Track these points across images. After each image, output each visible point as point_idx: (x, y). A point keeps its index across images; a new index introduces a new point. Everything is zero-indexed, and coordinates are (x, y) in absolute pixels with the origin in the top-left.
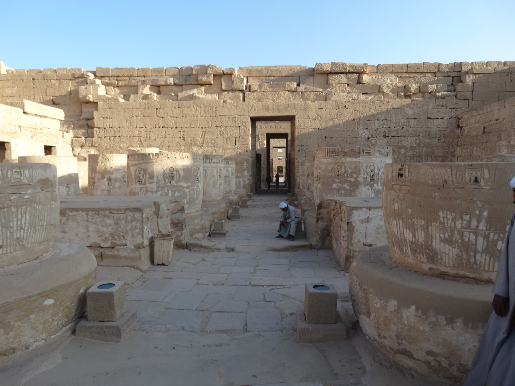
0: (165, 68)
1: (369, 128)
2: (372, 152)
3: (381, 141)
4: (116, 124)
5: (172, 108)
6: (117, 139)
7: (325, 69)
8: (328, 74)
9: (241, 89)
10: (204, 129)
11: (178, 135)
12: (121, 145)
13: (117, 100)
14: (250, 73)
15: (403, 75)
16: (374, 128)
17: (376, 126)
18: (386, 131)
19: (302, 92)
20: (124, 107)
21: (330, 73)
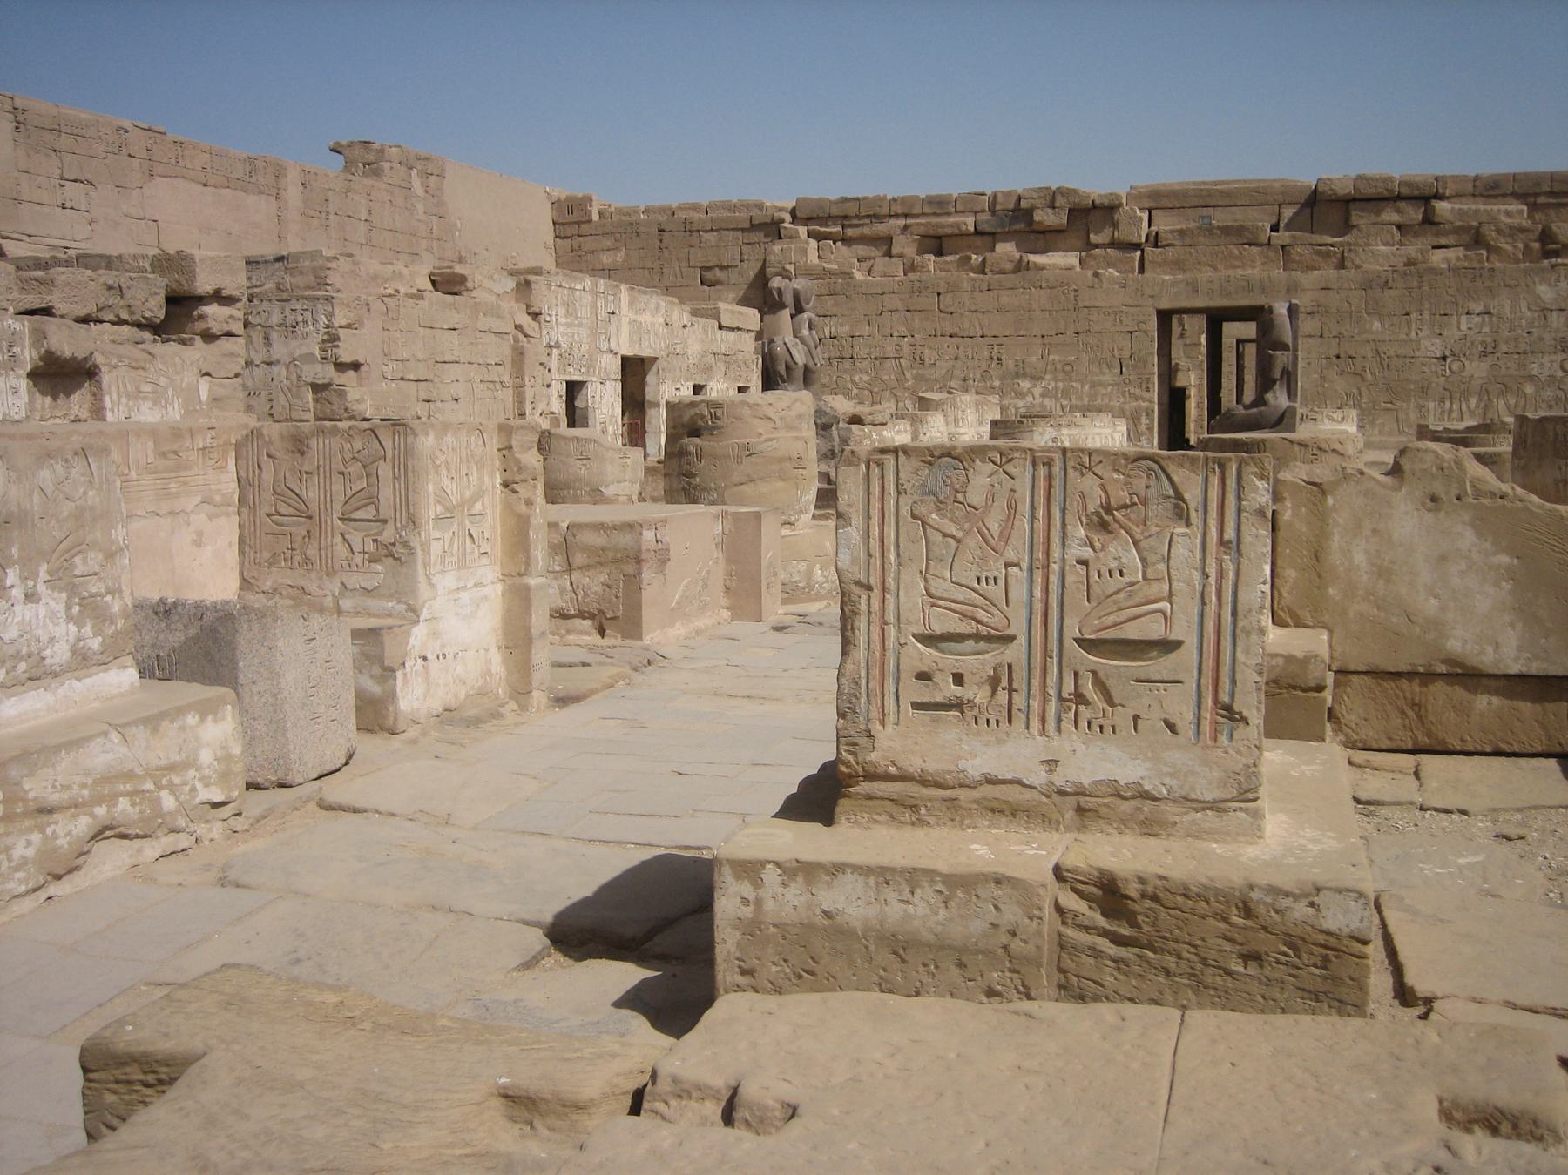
0: (955, 195)
1: (1445, 333)
2: (1319, 417)
3: (1475, 364)
4: (844, 330)
5: (973, 290)
6: (847, 364)
7: (1341, 192)
8: (1348, 201)
9: (1135, 240)
10: (1046, 340)
11: (986, 354)
12: (857, 378)
13: (850, 275)
14: (1158, 200)
15: (1541, 200)
16: (1457, 335)
17: (1464, 327)
18: (1489, 340)
19: (1283, 247)
20: (864, 290)
21: (1355, 200)
